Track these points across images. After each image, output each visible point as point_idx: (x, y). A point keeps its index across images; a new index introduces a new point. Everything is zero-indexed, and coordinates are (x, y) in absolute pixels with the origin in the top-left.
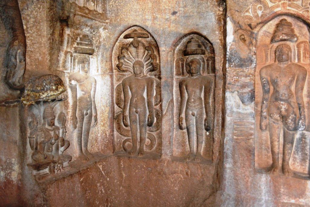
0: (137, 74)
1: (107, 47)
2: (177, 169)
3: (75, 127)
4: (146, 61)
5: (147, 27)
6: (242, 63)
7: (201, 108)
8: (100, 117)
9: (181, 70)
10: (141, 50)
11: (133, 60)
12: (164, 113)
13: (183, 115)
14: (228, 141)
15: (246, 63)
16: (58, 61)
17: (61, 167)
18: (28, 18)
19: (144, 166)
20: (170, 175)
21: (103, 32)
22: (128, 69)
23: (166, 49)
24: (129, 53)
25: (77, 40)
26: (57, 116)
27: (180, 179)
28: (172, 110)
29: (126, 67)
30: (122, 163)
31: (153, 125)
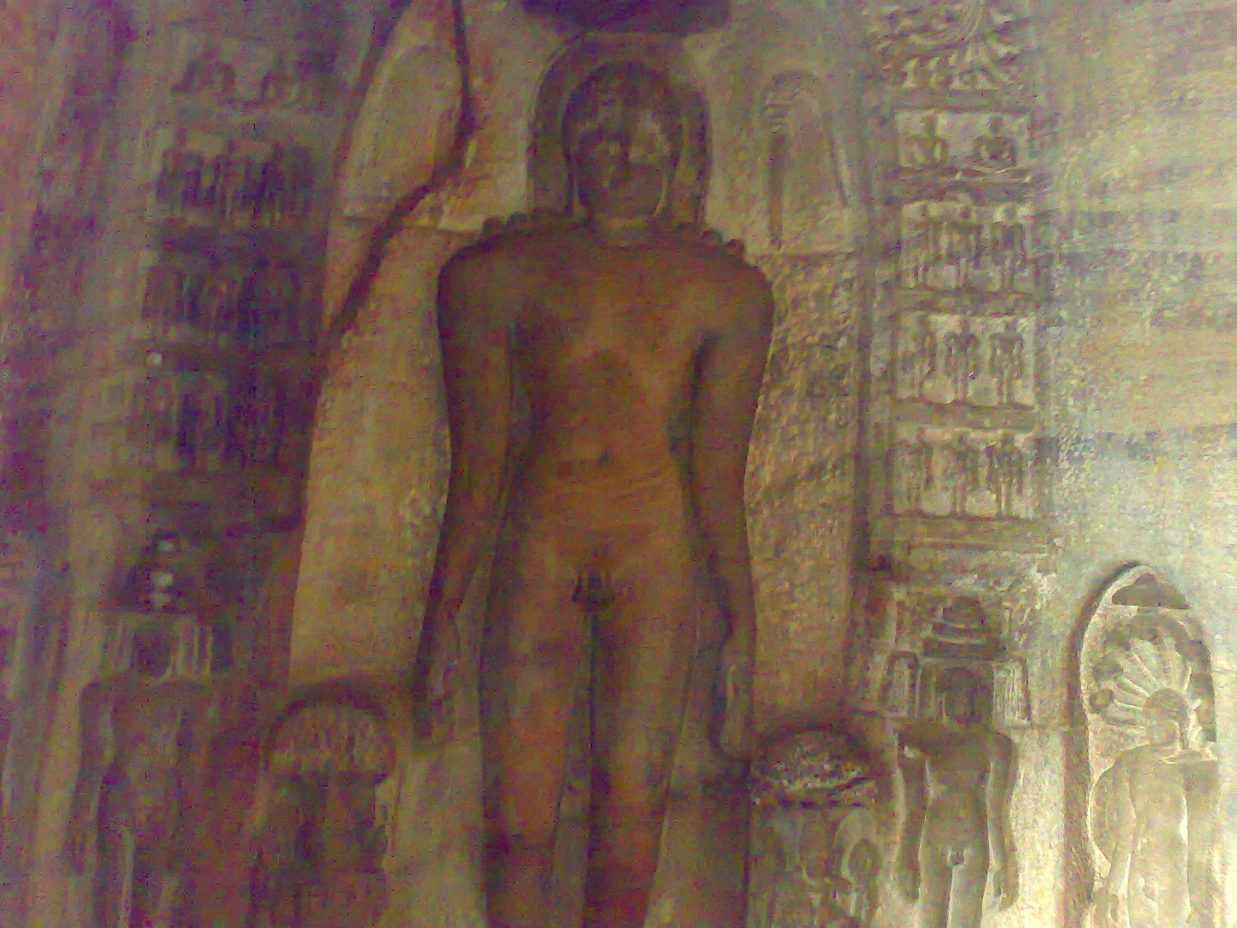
1: (1054, 632)
5: (1172, 572)
16: (866, 683)
18: (798, 559)
26: (850, 849)
29: (1128, 710)
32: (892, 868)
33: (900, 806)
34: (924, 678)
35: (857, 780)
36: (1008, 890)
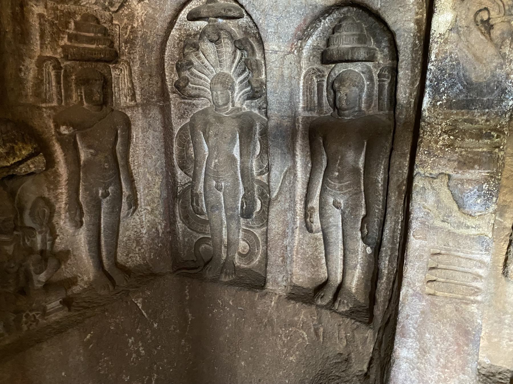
0: (219, 106)
1: (149, 42)
2: (296, 319)
3: (79, 224)
4: (239, 75)
6: (472, 95)
7: (356, 194)
8: (144, 195)
9: (316, 99)
10: (227, 48)
11: (212, 72)
12: (274, 195)
13: (315, 203)
14: (410, 298)
15: (484, 96)
16: (21, 82)
17: (37, 316)
19: (231, 303)
20: (281, 328)
21: (140, 5)
22: (202, 93)
23: (279, 47)
24: (201, 55)
25: (67, 28)
26: (29, 205)
27: (300, 340)
28: (293, 188)
29: (196, 89)
30: (188, 290)
31: (254, 216)
32: (63, 212)
33: (63, 169)
34: (66, 76)
35: (30, 156)
36: (134, 203)
